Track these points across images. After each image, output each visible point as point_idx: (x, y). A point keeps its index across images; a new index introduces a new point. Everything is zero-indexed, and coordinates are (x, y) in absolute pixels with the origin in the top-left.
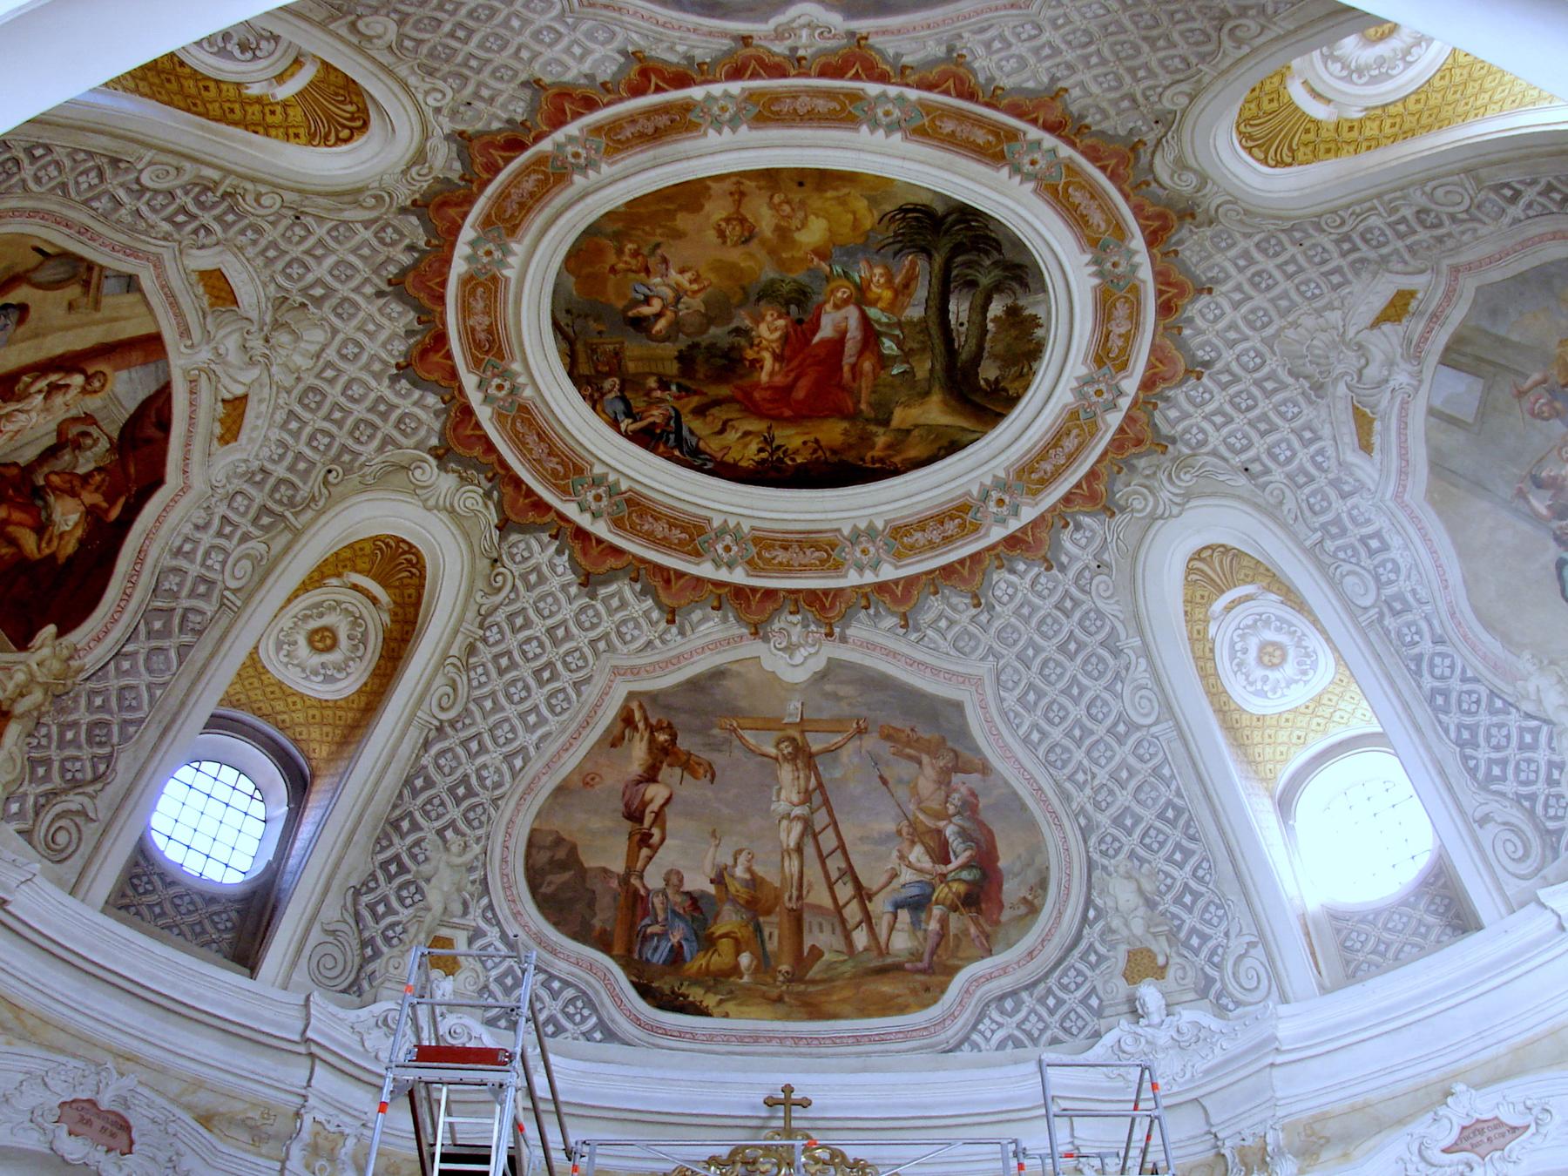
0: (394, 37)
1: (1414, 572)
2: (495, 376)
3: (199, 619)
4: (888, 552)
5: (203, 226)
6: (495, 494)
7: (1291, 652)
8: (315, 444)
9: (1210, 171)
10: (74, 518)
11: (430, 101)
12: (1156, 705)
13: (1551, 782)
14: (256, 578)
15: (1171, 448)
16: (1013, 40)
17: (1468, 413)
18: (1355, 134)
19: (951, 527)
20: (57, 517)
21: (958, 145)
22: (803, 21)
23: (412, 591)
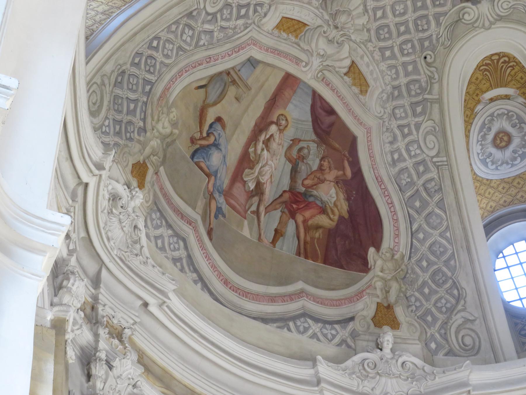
3: (433, 183)
5: (256, 5)
8: (406, 52)
10: (333, 191)
14: (442, 141)
20: (325, 198)
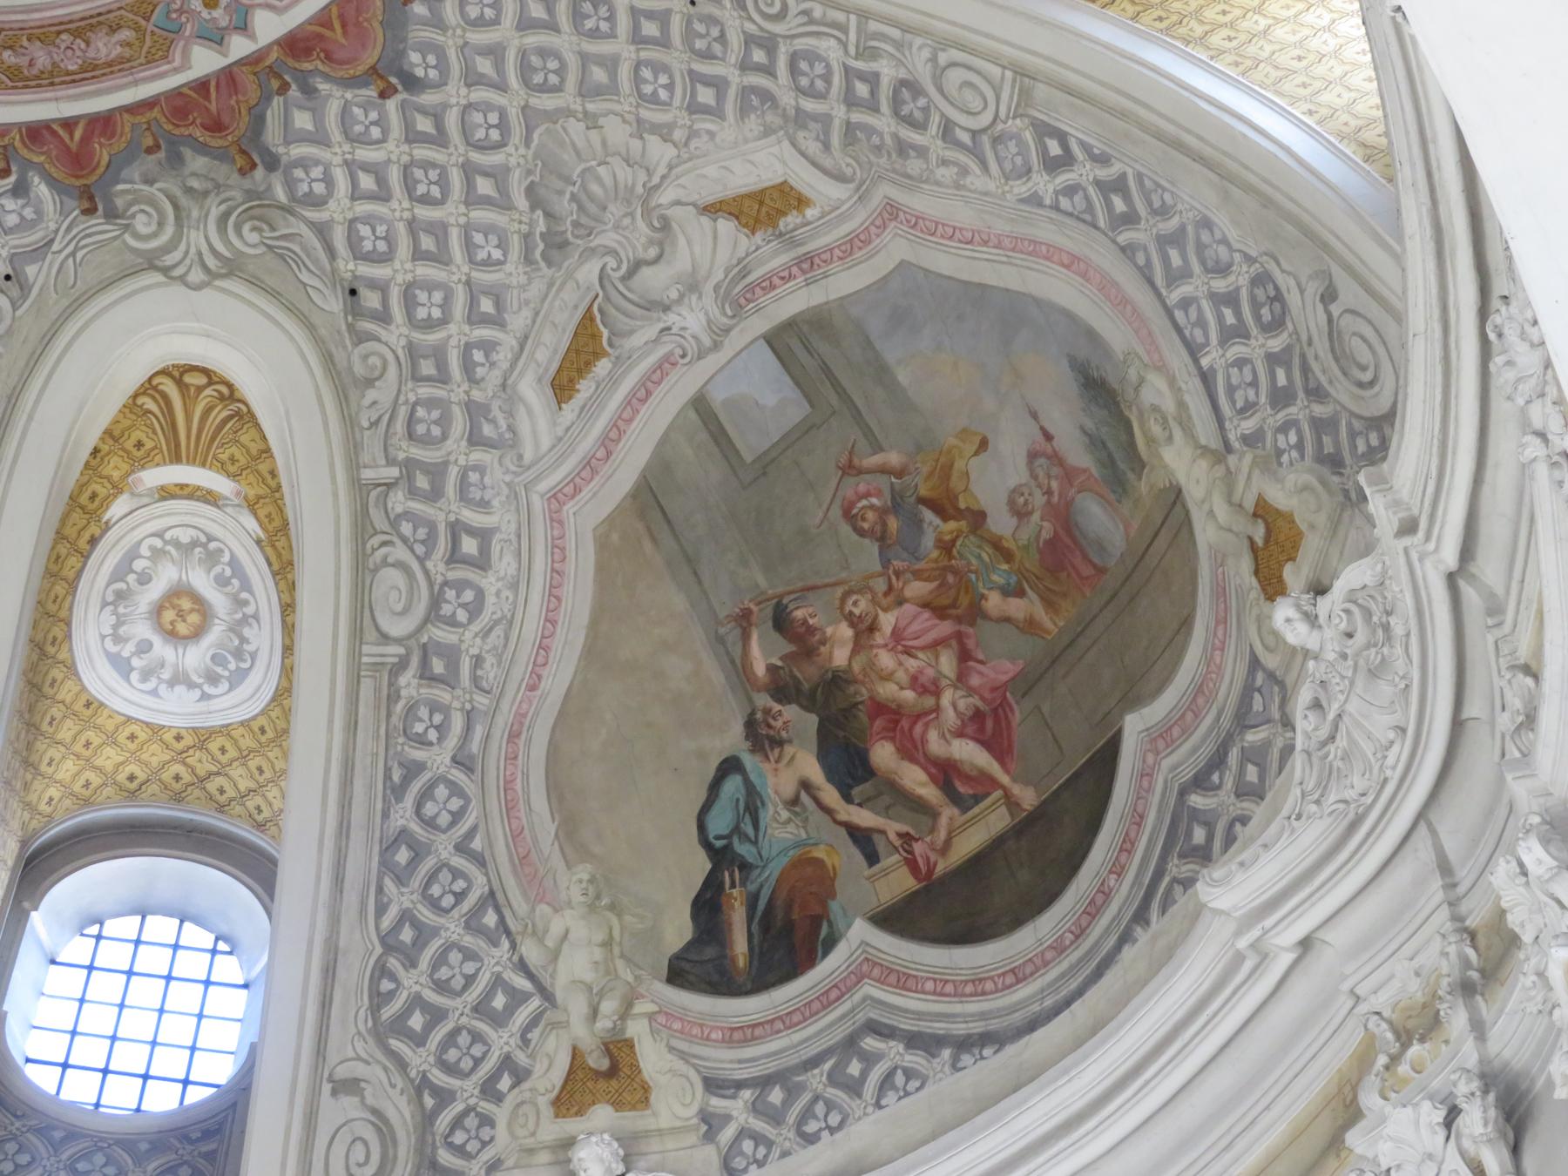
1: (499, 631)
7: (216, 633)
13: (489, 1090)
15: (259, 172)
17: (750, 445)
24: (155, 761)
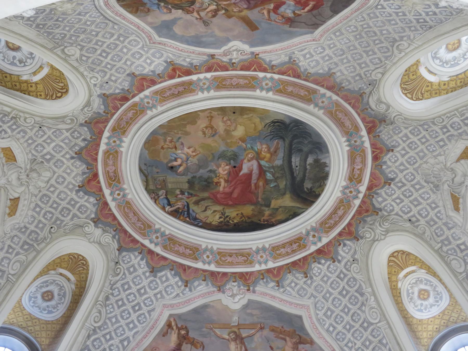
0: (79, 56)
2: (117, 190)
4: (270, 257)
5: (3, 130)
6: (117, 237)
7: (432, 293)
8: (46, 217)
9: (391, 103)
11: (92, 81)
12: (379, 315)
15: (380, 213)
16: (314, 54)
18: (446, 86)
19: (295, 246)
21: (294, 96)
22: (234, 48)
23: (84, 275)
24: (438, 323)
